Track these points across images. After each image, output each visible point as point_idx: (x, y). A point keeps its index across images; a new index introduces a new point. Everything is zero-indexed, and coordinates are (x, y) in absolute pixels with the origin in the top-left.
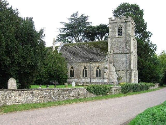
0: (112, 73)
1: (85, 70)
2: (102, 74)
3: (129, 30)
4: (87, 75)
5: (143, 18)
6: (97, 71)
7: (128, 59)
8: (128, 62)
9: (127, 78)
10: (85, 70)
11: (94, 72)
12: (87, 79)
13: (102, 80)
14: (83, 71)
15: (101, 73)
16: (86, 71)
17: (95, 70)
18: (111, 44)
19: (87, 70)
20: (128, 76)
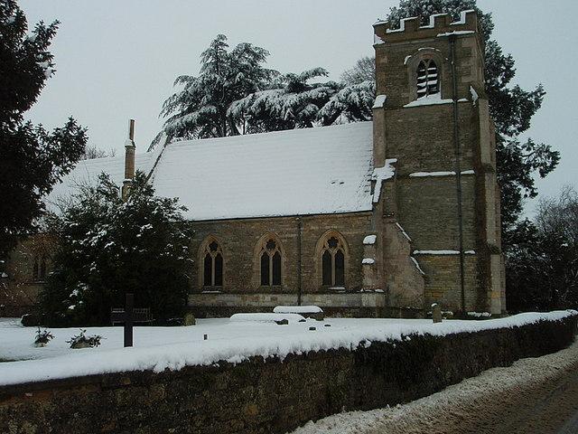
0: (396, 267)
1: (271, 254)
2: (351, 270)
3: (469, 74)
4: (284, 276)
5: (531, 121)
6: (327, 256)
7: (468, 203)
8: (469, 214)
9: (466, 286)
10: (271, 254)
11: (312, 263)
12: (284, 293)
13: (353, 297)
14: (265, 259)
15: (347, 265)
16: (277, 258)
17: (320, 250)
18: (387, 135)
19: (283, 253)
20: (470, 277)
